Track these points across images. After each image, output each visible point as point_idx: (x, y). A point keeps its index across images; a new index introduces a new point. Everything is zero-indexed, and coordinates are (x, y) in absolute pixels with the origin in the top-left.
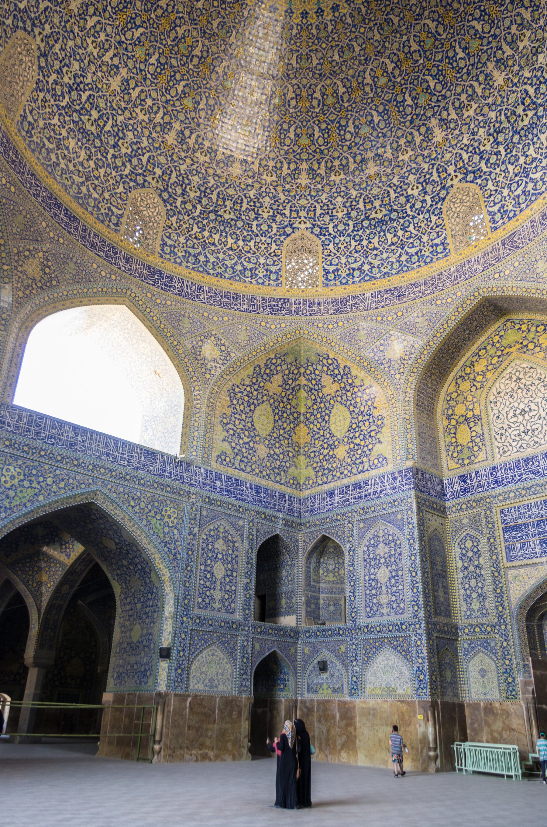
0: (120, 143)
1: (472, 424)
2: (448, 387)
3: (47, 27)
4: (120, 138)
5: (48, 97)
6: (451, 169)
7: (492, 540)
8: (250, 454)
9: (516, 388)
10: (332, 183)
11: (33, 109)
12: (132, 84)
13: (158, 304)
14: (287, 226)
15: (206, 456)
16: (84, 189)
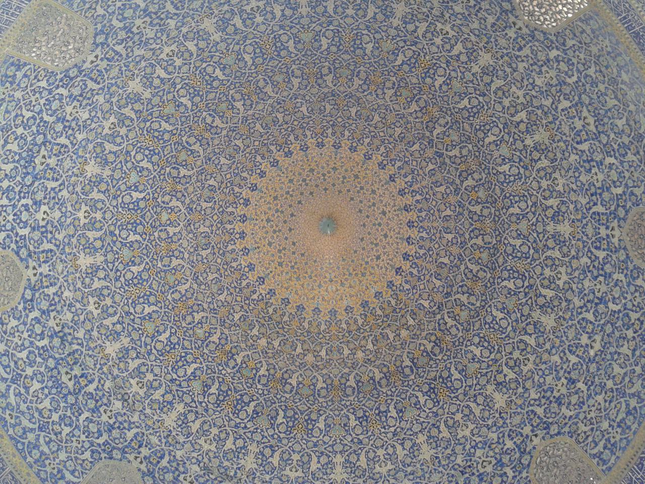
6: (45, 269)
10: (107, 115)
12: (380, 17)
14: (106, 39)
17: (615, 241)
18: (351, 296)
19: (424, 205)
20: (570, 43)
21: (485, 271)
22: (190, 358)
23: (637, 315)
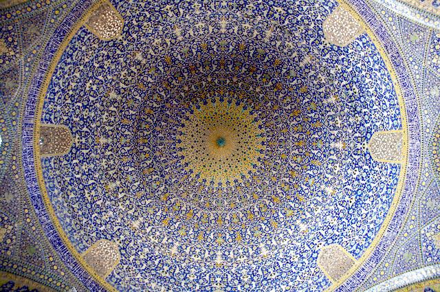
3: (121, 236)
6: (359, 146)
10: (318, 215)
12: (184, 247)
17: (78, 136)
19: (172, 151)
20: (94, 234)
23: (67, 102)
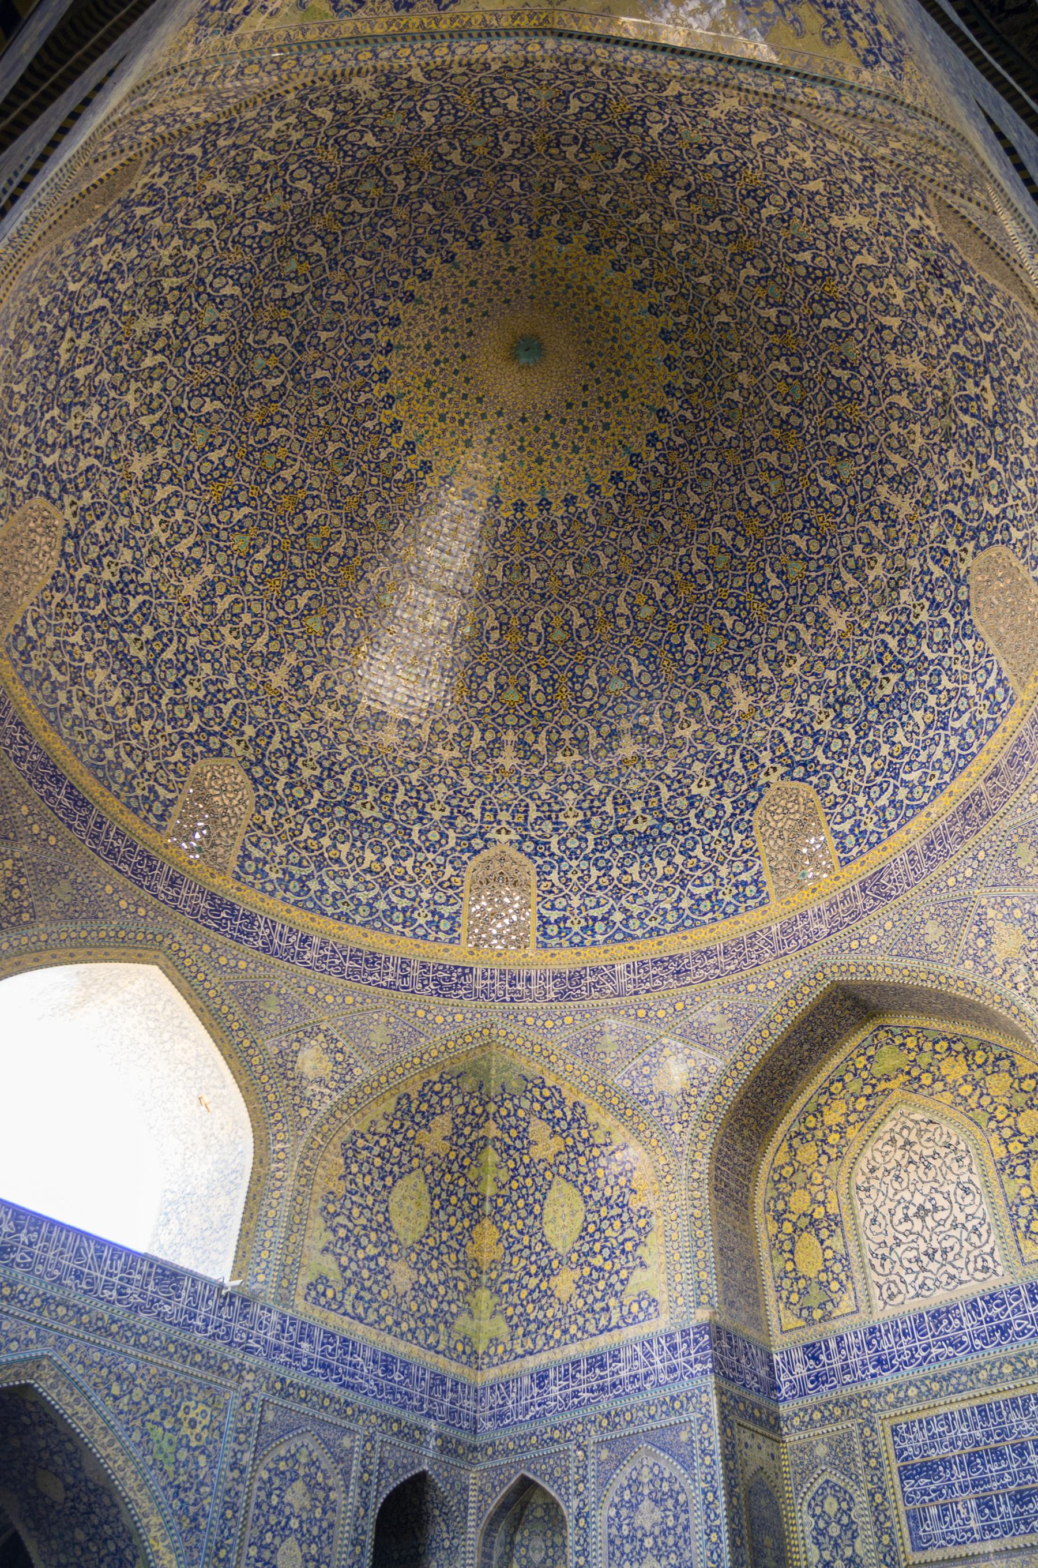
0: (186, 681)
1: (824, 1234)
2: (774, 1154)
3: (87, 495)
4: (187, 672)
5: (70, 600)
6: (765, 757)
7: (879, 1498)
8: (376, 1282)
9: (904, 1162)
10: (558, 768)
11: (39, 618)
12: (220, 589)
13: (221, 967)
14: (474, 836)
15: (285, 1283)
16: (109, 753)
18: (597, 272)
21: (387, 169)
22: (814, 492)
